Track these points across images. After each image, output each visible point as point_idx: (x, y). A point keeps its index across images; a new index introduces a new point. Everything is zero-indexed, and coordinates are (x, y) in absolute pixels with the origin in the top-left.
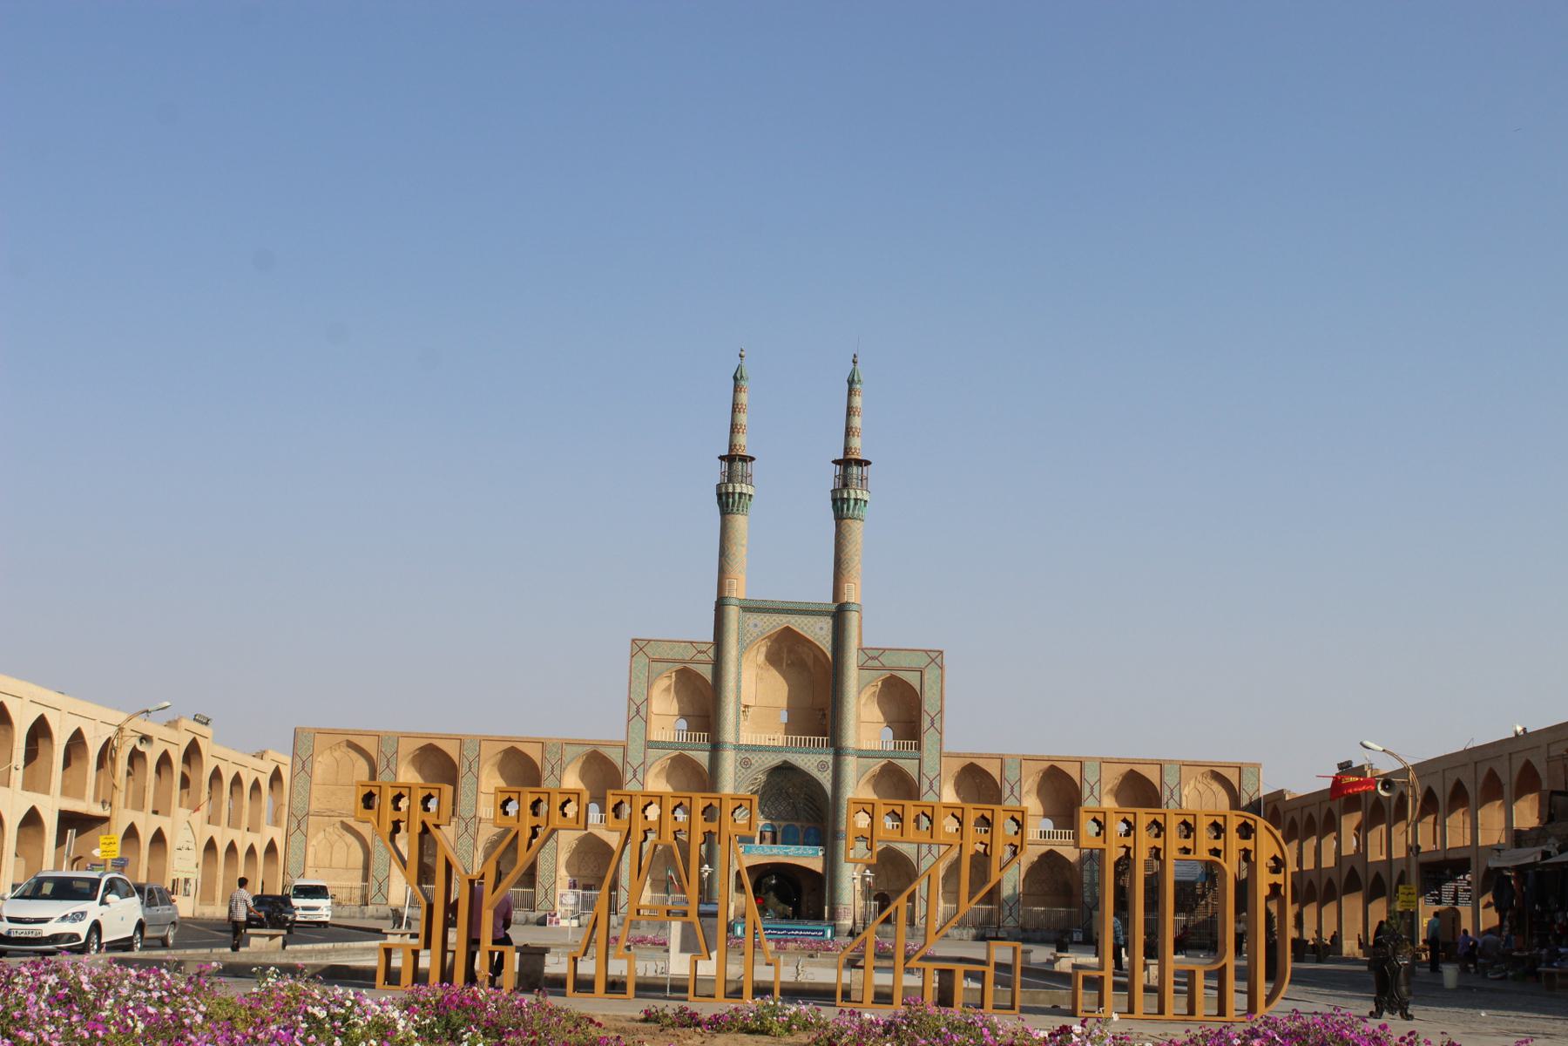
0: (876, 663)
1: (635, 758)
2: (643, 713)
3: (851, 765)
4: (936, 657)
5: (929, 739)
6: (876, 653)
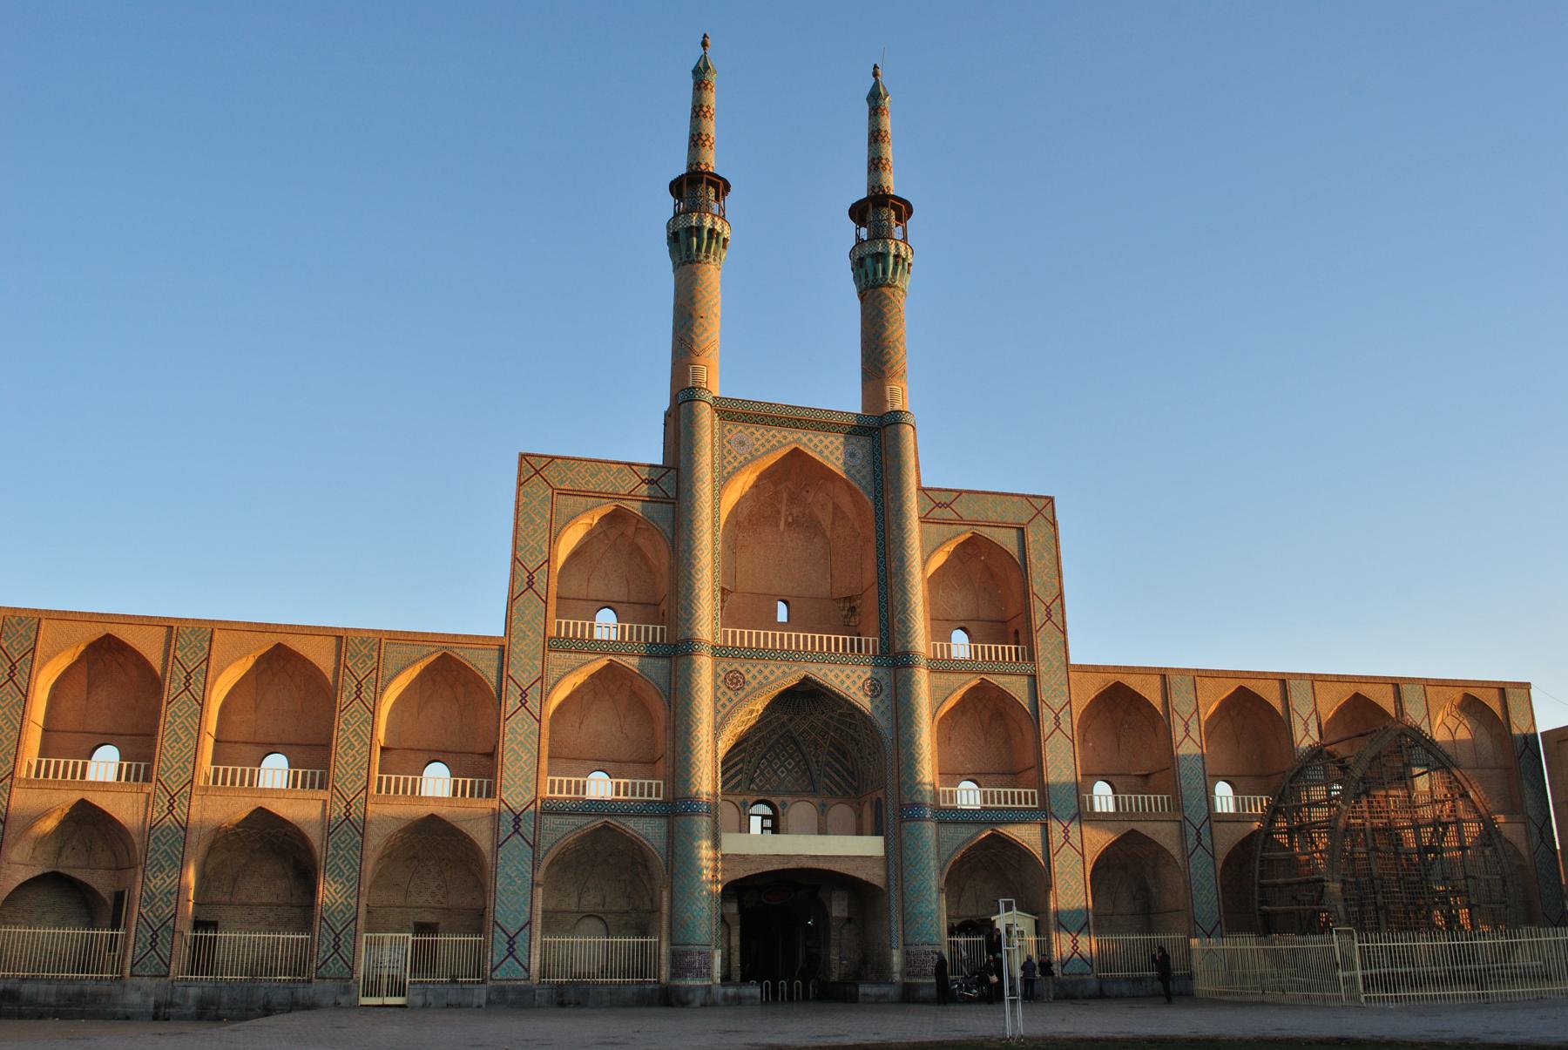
0: (947, 514)
1: (523, 669)
2: (540, 585)
3: (923, 681)
4: (1044, 507)
5: (1043, 642)
6: (945, 498)
